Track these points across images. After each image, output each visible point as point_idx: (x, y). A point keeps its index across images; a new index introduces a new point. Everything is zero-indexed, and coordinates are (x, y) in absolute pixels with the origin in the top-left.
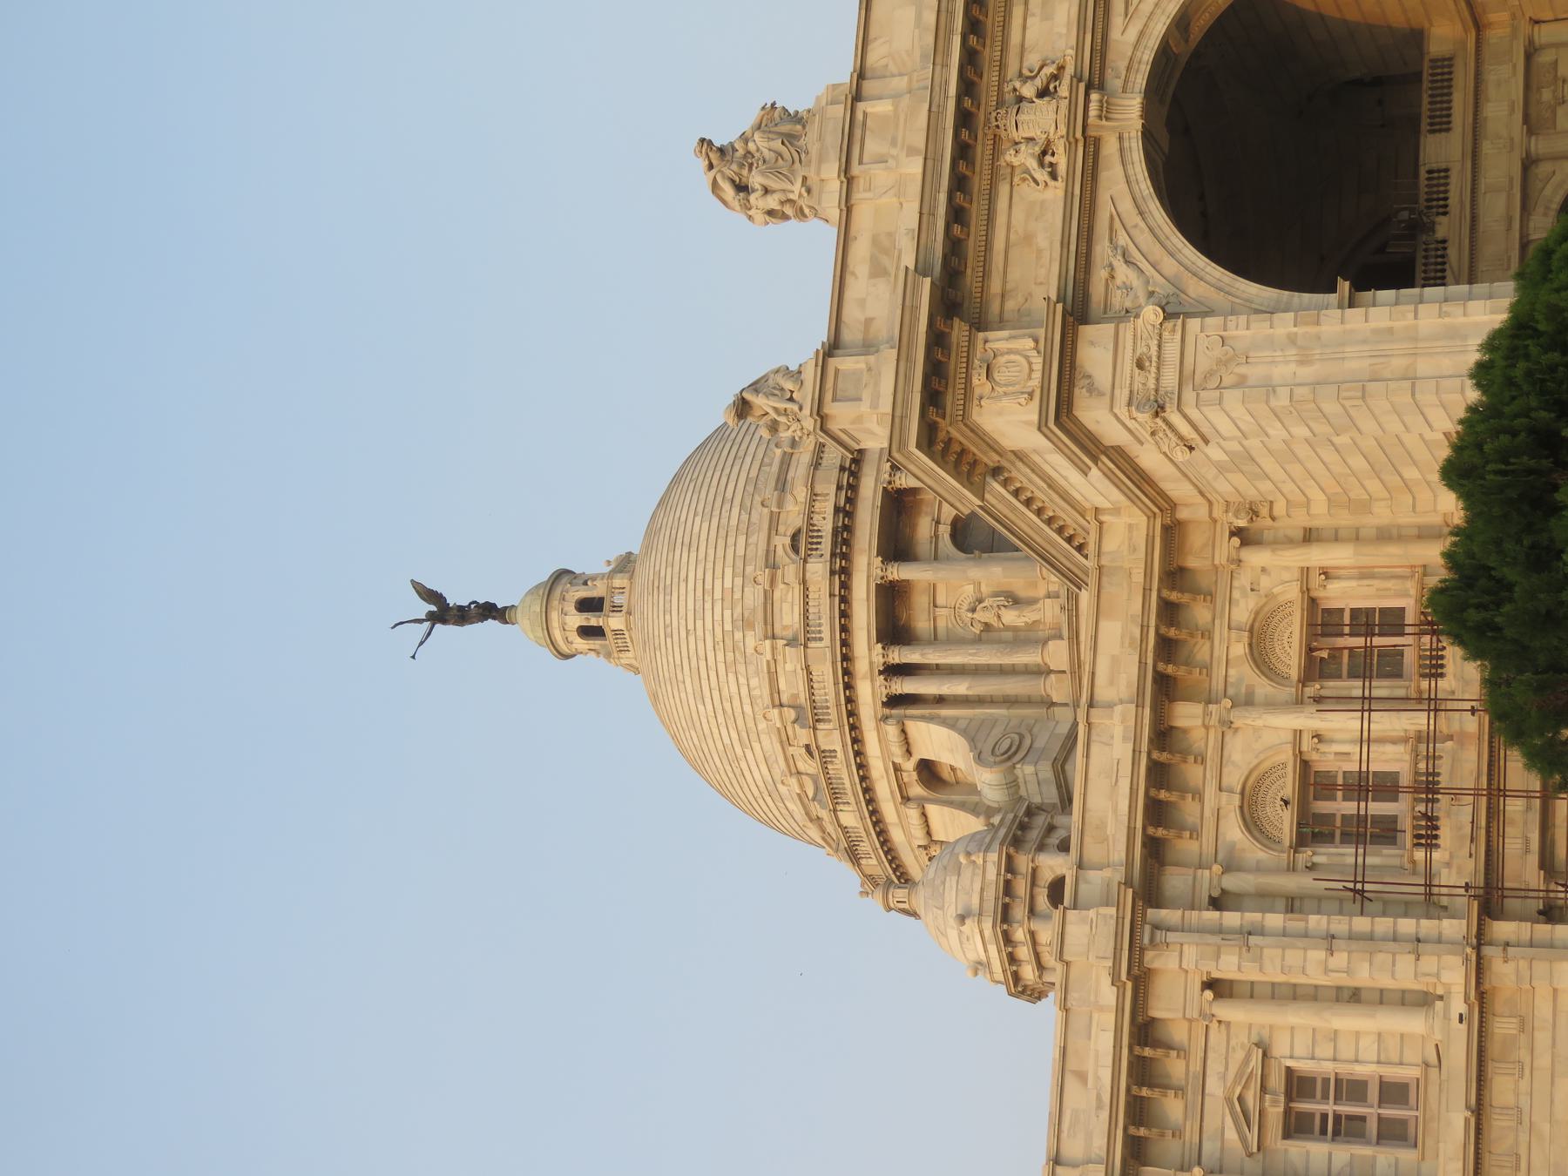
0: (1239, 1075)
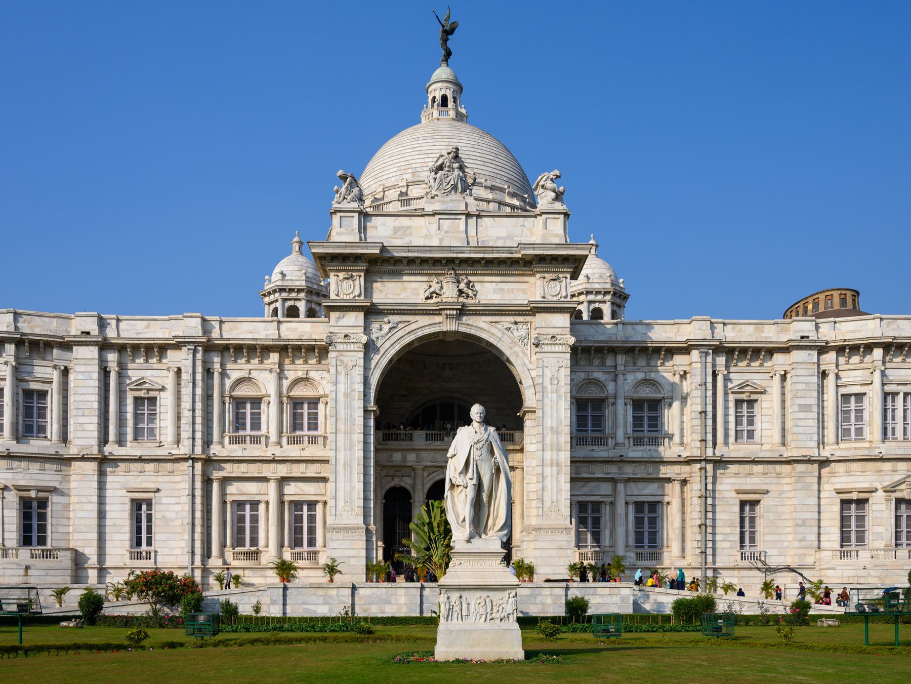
0: (152, 381)
